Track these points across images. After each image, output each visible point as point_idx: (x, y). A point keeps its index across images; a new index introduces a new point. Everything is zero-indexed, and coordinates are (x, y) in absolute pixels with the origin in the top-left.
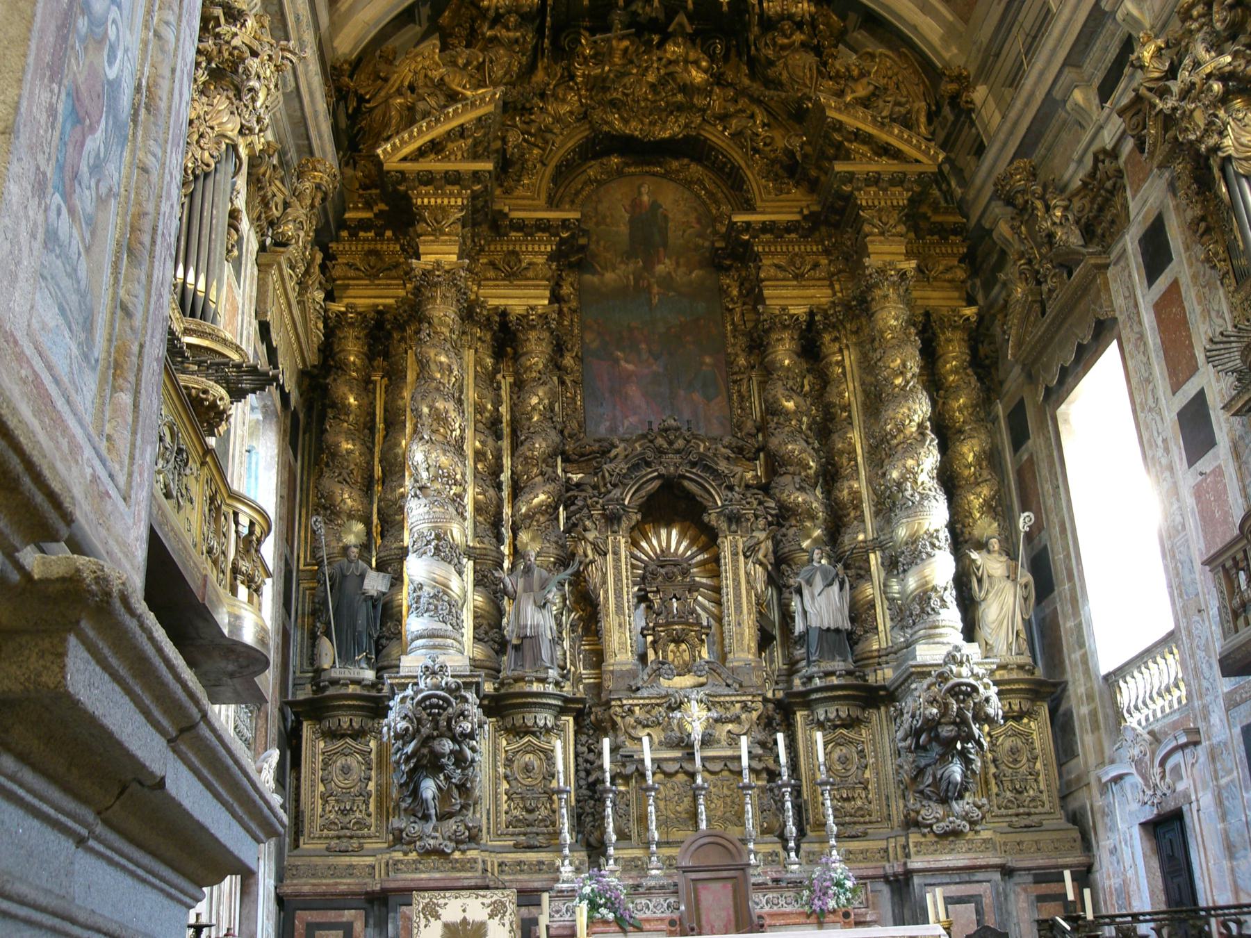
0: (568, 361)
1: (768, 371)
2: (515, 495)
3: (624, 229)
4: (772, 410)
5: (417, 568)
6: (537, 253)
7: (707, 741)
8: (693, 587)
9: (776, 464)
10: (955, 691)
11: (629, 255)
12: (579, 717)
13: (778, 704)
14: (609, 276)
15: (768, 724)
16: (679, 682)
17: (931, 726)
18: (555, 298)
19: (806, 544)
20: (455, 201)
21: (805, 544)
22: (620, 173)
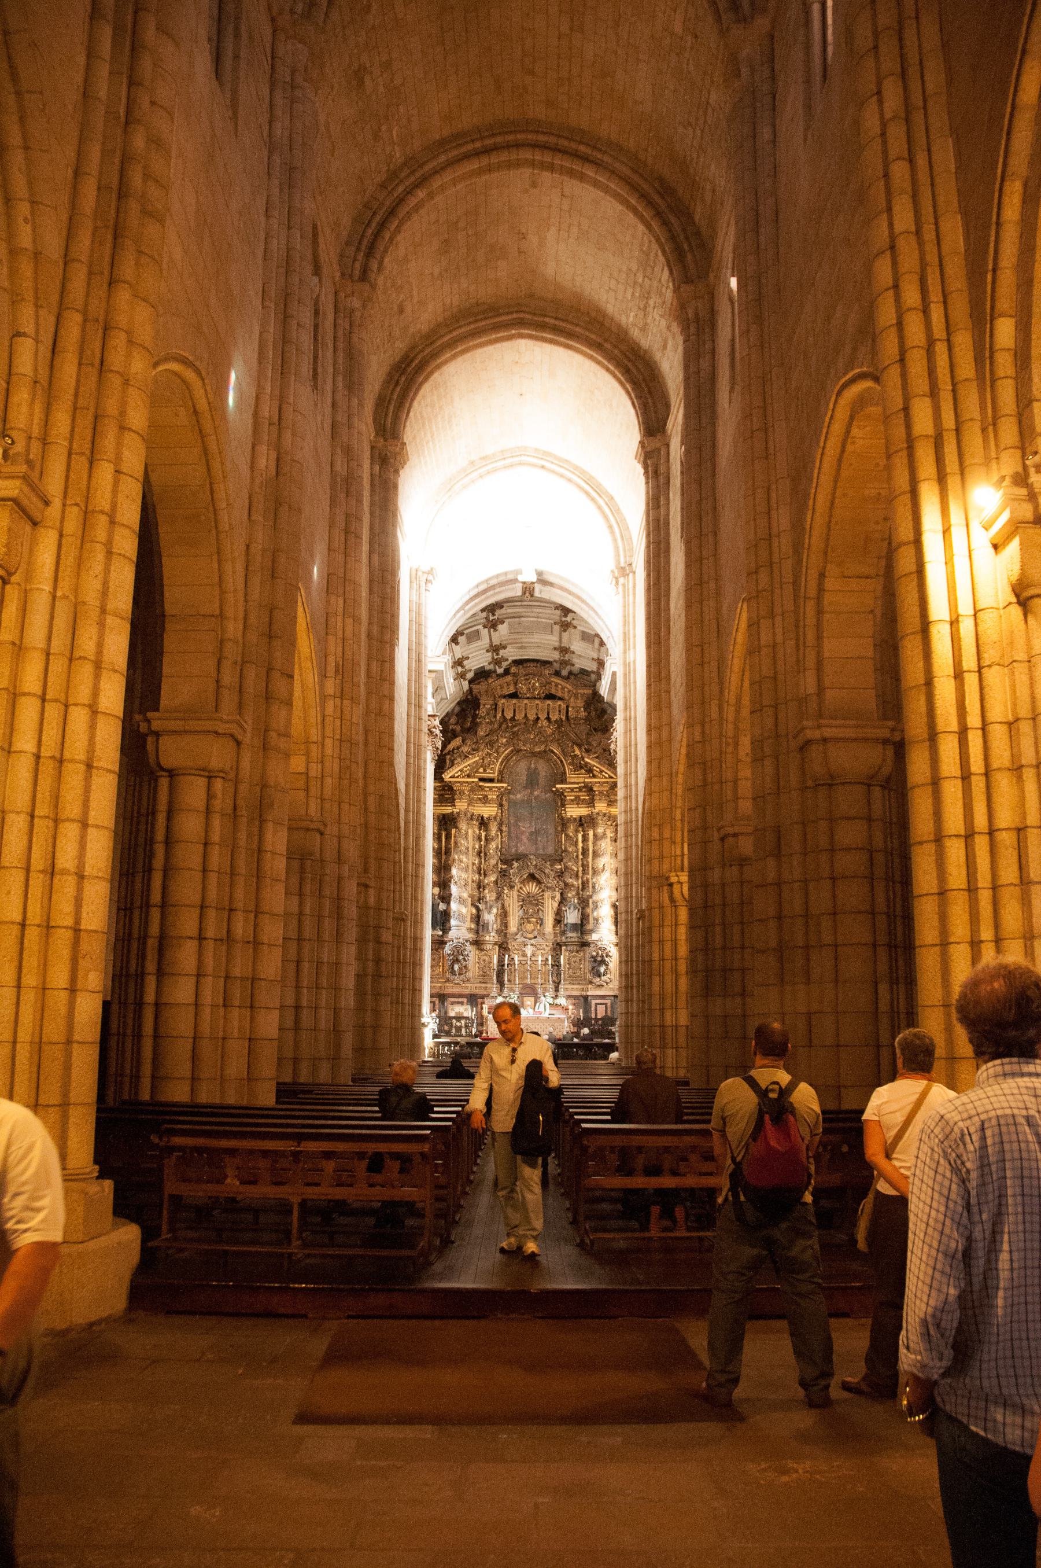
0: (504, 828)
1: (567, 835)
2: (485, 875)
3: (525, 778)
4: (566, 851)
5: (454, 906)
6: (492, 796)
7: (534, 955)
8: (537, 905)
9: (566, 868)
10: (600, 949)
11: (525, 788)
12: (500, 946)
13: (558, 944)
14: (519, 796)
15: (555, 949)
16: (531, 936)
17: (593, 957)
18: (501, 805)
19: (570, 895)
20: (466, 789)
21: (570, 895)
22: (525, 757)
